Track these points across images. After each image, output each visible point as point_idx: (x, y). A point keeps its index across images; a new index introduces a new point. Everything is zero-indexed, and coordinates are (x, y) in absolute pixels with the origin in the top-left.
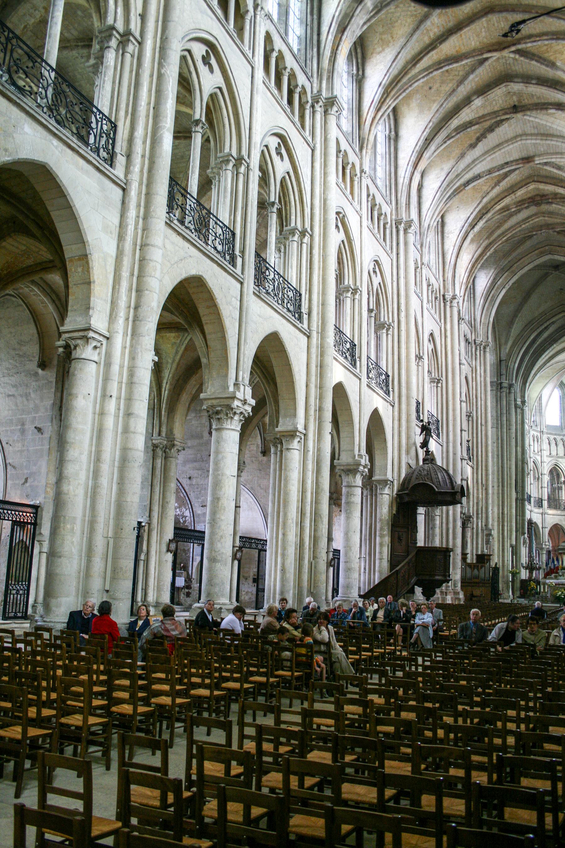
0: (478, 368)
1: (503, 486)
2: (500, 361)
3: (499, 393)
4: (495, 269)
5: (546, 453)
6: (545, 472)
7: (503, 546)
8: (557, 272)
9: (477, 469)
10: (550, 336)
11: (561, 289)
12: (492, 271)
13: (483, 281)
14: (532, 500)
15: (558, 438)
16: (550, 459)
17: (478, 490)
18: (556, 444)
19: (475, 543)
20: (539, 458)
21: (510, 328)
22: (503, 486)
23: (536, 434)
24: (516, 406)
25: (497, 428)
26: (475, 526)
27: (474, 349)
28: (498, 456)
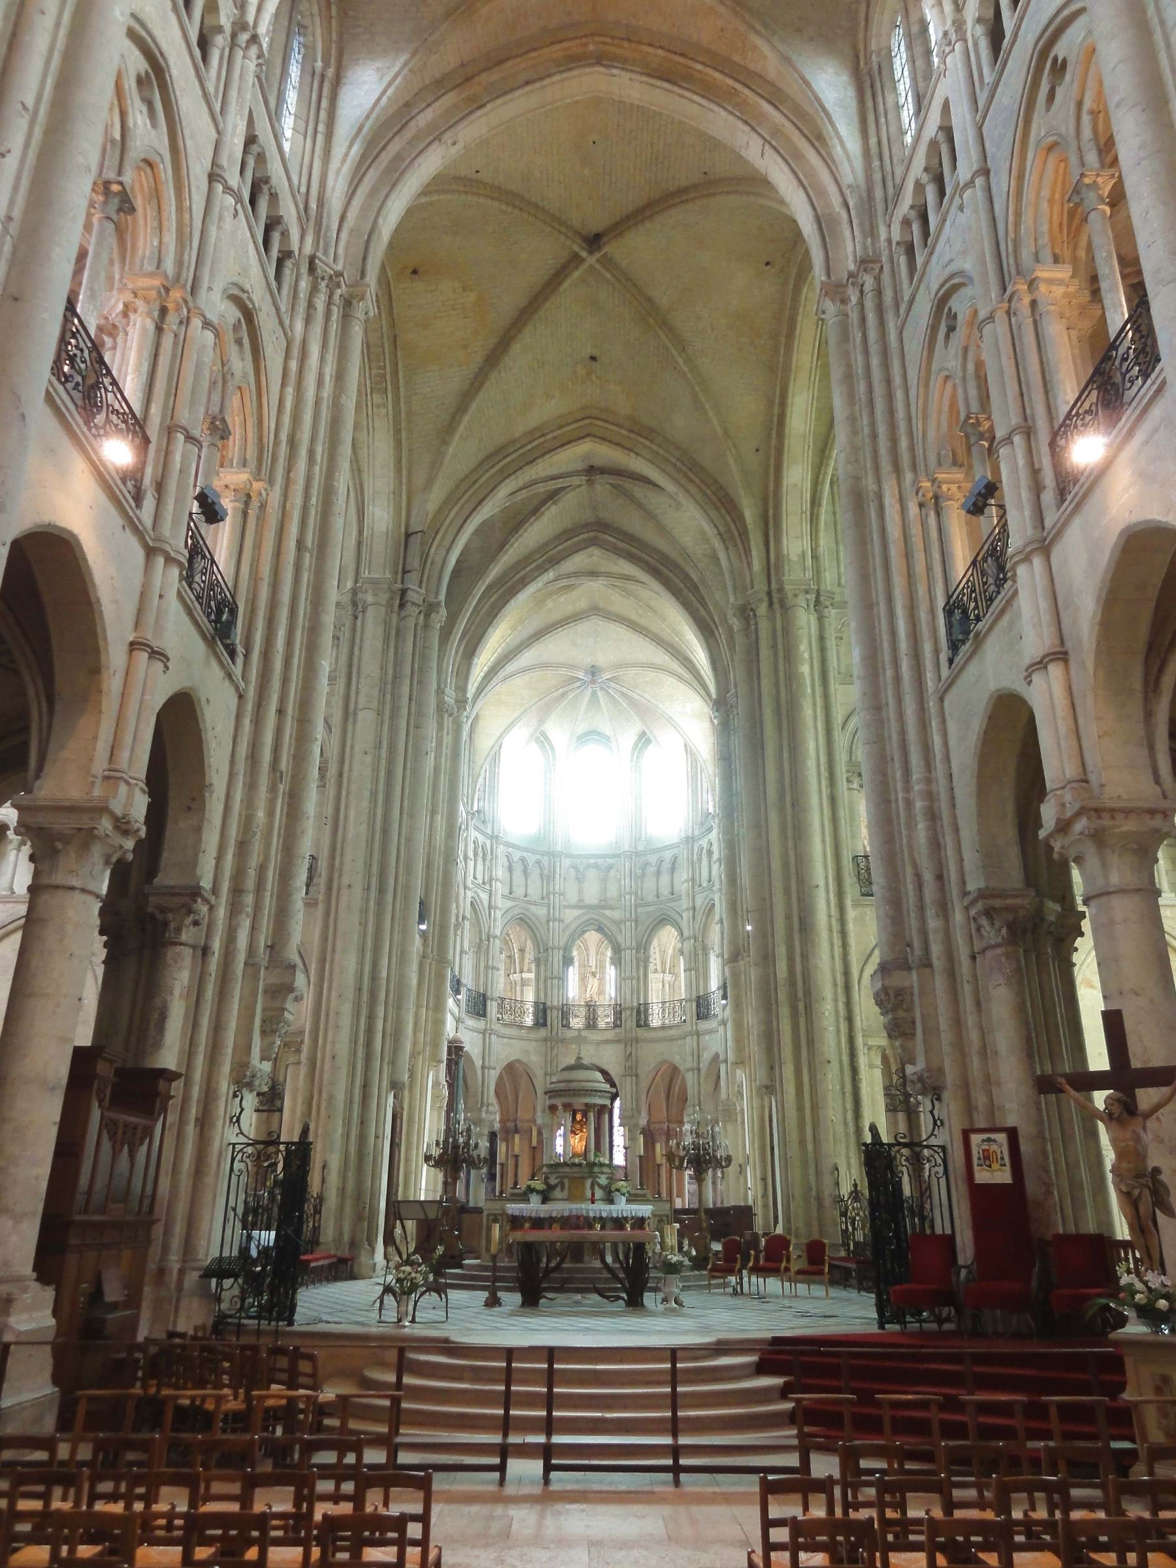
0: (315, 350)
1: (382, 890)
2: (408, 535)
3: (395, 617)
4: (414, 54)
5: (500, 889)
6: (498, 933)
7: (366, 1086)
8: (592, 260)
9: (260, 706)
10: (542, 548)
11: (593, 358)
12: (403, 58)
13: (367, 88)
14: (463, 990)
15: (531, 859)
16: (509, 904)
17: (251, 787)
18: (526, 873)
19: (205, 1022)
20: (484, 896)
21: (445, 443)
22: (382, 890)
23: (481, 839)
24: (441, 709)
25: (380, 713)
26: (216, 945)
27: (304, 284)
28: (374, 794)
